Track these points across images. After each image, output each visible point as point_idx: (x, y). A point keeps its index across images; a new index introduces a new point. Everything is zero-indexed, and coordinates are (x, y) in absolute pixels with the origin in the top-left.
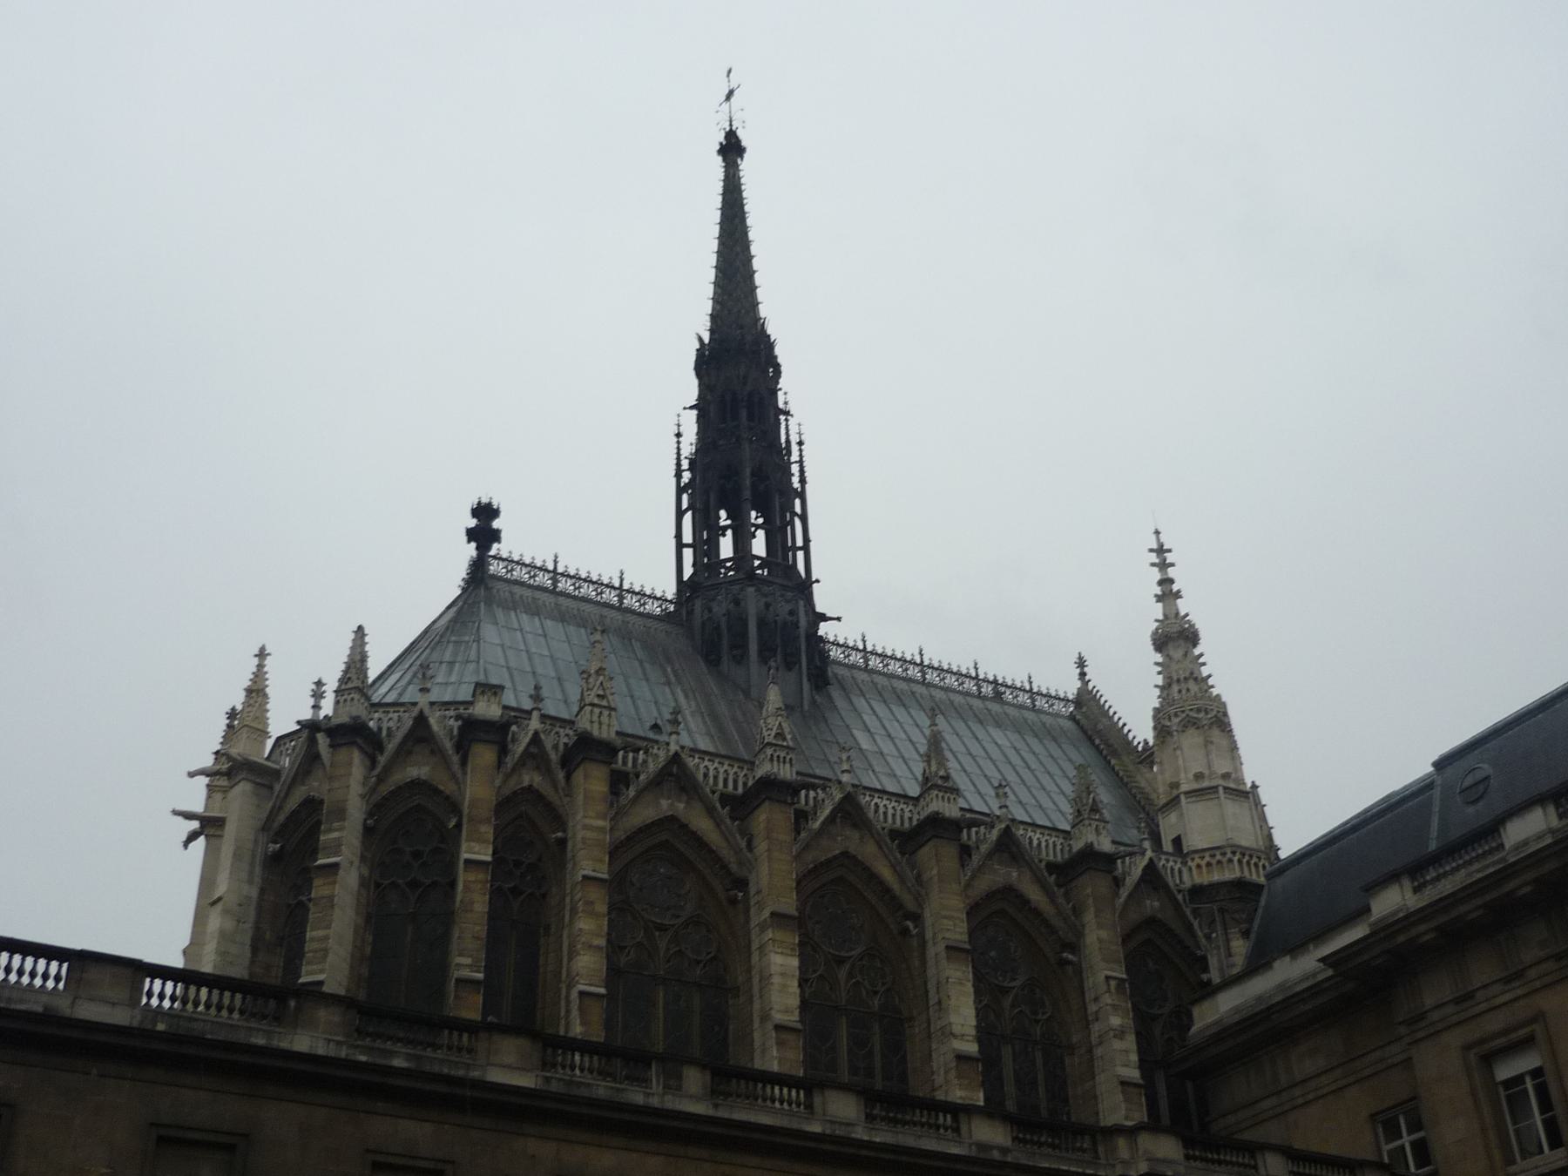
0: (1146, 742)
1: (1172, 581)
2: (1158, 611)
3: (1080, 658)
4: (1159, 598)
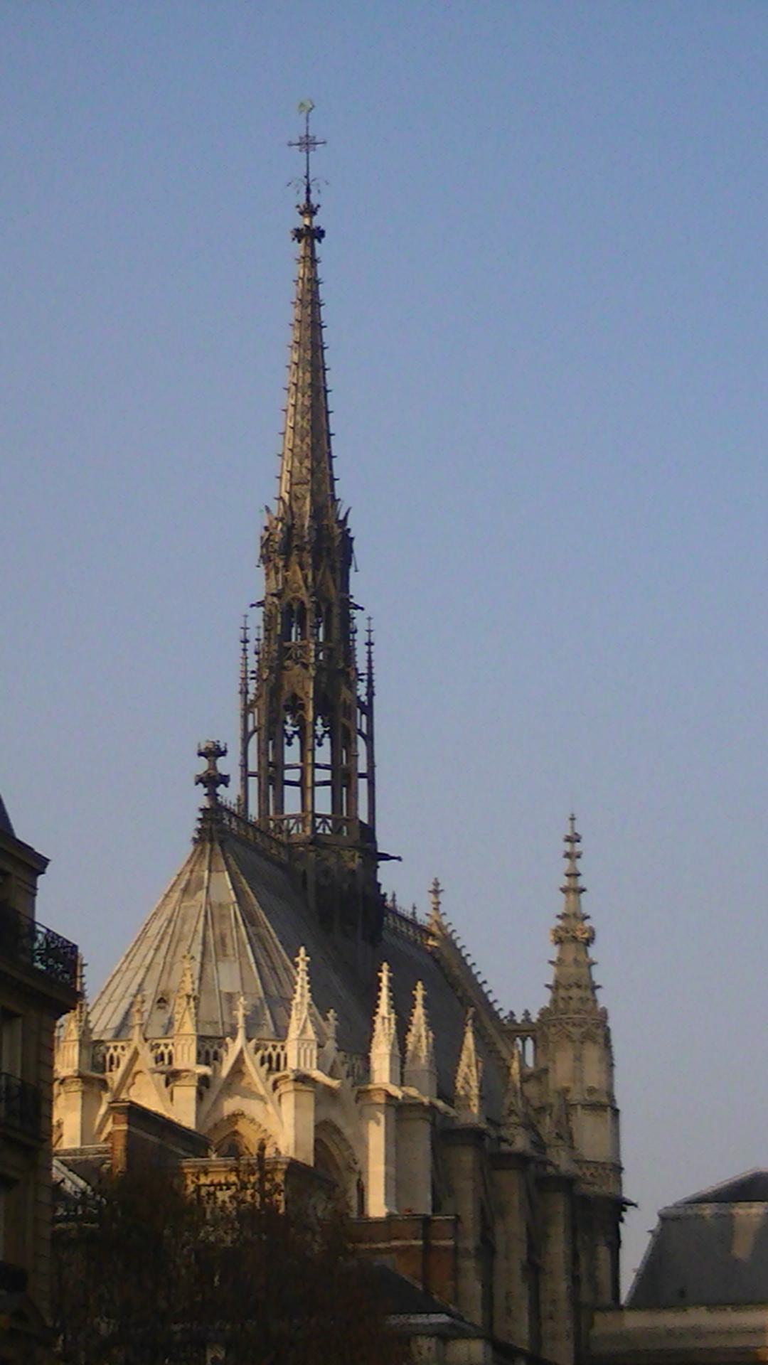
0: (512, 1014)
1: (579, 875)
2: (560, 904)
3: (437, 884)
4: (565, 890)
